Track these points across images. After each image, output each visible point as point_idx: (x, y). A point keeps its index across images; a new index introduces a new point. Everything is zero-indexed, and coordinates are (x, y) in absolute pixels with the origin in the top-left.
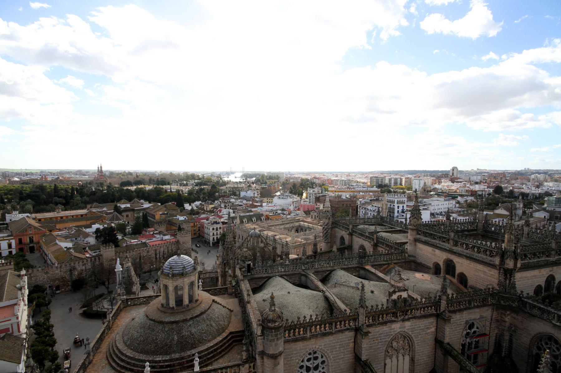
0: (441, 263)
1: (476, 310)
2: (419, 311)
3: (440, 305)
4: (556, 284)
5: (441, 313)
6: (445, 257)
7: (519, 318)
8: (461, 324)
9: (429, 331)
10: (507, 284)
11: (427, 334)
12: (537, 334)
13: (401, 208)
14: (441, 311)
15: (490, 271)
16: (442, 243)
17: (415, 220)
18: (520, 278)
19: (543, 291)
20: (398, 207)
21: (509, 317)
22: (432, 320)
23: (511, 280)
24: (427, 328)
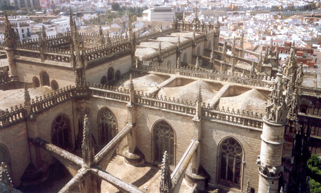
0: (38, 77)
2: (6, 121)
4: (115, 73)
6: (40, 71)
7: (90, 102)
9: (20, 134)
10: (80, 80)
11: (18, 137)
13: (26, 32)
15: (70, 73)
18: (89, 74)
19: (107, 80)
20: (23, 31)
21: (84, 104)
22: (23, 125)
24: (19, 132)
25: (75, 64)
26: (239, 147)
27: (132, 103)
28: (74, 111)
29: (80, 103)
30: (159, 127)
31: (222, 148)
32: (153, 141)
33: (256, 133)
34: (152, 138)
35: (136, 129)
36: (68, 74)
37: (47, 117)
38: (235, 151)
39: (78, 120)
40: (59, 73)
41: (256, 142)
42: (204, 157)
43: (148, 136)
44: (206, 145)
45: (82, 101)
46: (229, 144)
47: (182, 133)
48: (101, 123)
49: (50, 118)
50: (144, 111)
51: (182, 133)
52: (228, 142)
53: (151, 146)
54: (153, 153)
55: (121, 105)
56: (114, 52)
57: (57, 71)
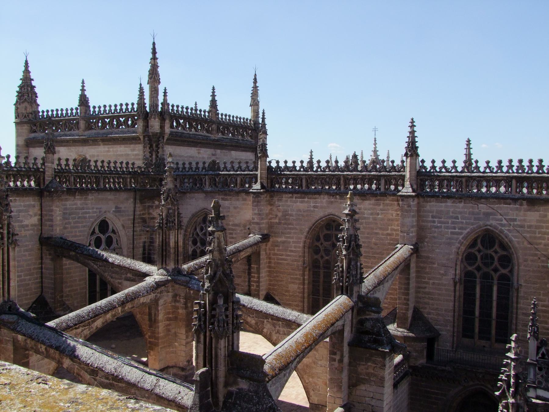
1: (109, 196)
3: (44, 172)
5: (48, 185)
8: (85, 218)
9: (26, 222)
12: (191, 219)
14: (47, 183)
15: (133, 150)
16: (69, 133)
17: (26, 104)
23: (158, 152)
25: (146, 126)
26: (505, 253)
27: (263, 187)
28: (136, 221)
29: (149, 207)
30: (322, 237)
31: (464, 259)
32: (307, 273)
33: (542, 208)
34: (305, 265)
35: (270, 250)
36: (130, 153)
37: (83, 209)
38: (496, 263)
39: (141, 245)
40: (111, 153)
41: (544, 230)
42: (425, 288)
43: (296, 261)
44: (428, 257)
45: (154, 203)
46: (481, 248)
47: (373, 240)
48: (190, 253)
49: (87, 215)
50: (289, 203)
51: (373, 240)
52: (479, 245)
53: (302, 287)
54: (306, 300)
55: (238, 200)
56: (222, 132)
57: (108, 151)
